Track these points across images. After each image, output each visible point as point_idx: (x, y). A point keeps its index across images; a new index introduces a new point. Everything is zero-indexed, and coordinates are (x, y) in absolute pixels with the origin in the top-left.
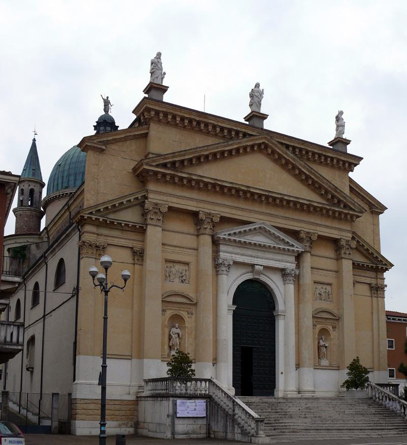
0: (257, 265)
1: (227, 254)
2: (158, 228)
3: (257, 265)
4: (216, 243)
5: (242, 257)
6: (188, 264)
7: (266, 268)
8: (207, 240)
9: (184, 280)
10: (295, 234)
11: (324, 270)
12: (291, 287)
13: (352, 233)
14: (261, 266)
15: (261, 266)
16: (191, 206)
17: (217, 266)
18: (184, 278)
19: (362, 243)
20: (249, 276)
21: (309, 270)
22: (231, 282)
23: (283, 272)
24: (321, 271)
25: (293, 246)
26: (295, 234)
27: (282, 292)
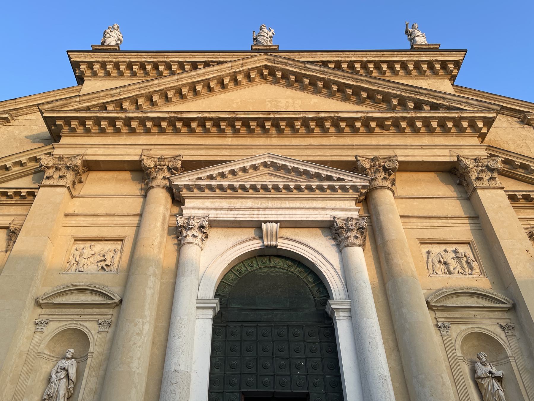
0: (265, 222)
1: (195, 208)
2: (58, 190)
3: (265, 222)
4: (177, 199)
5: (233, 212)
6: (122, 240)
7: (285, 224)
8: (160, 198)
9: (107, 265)
10: (353, 167)
11: (440, 217)
12: (360, 256)
13: (487, 149)
14: (276, 222)
15: (276, 222)
16: (131, 155)
17: (178, 233)
18: (108, 262)
19: (518, 161)
20: (256, 245)
21: (399, 221)
22: (212, 258)
23: (332, 230)
24: (434, 221)
25: (329, 178)
26: (353, 167)
27: (337, 263)
